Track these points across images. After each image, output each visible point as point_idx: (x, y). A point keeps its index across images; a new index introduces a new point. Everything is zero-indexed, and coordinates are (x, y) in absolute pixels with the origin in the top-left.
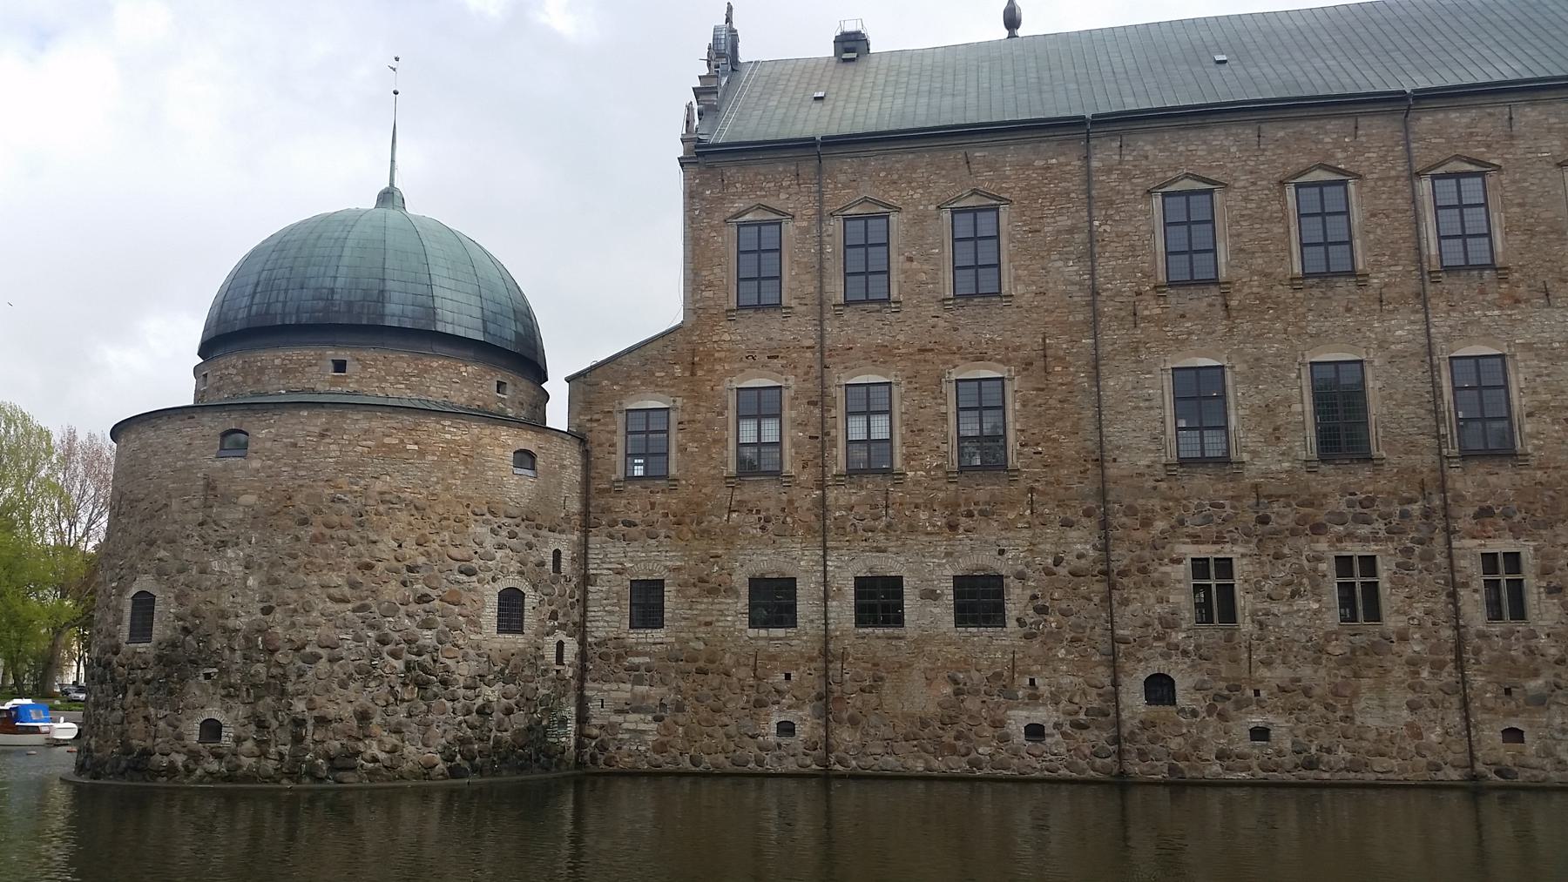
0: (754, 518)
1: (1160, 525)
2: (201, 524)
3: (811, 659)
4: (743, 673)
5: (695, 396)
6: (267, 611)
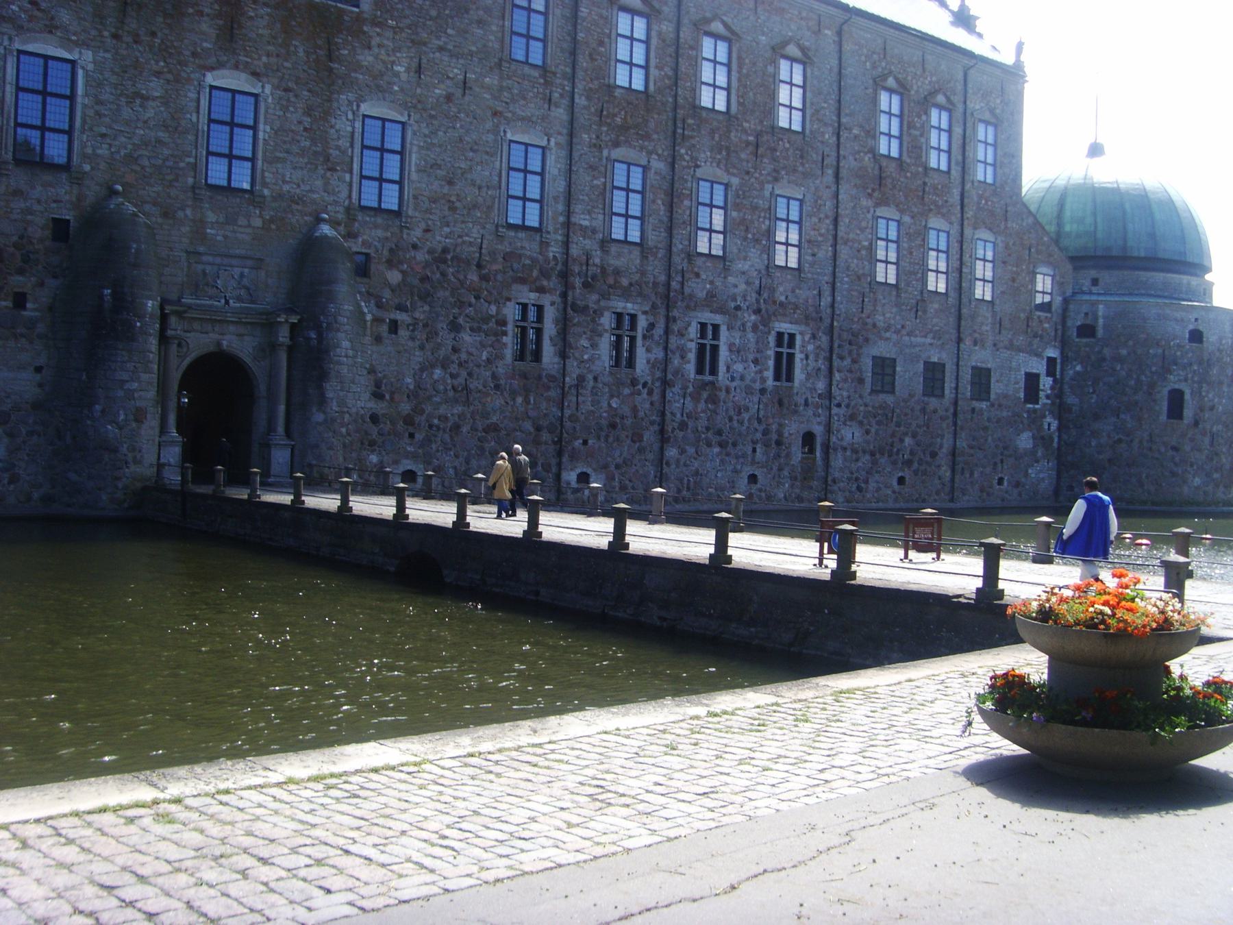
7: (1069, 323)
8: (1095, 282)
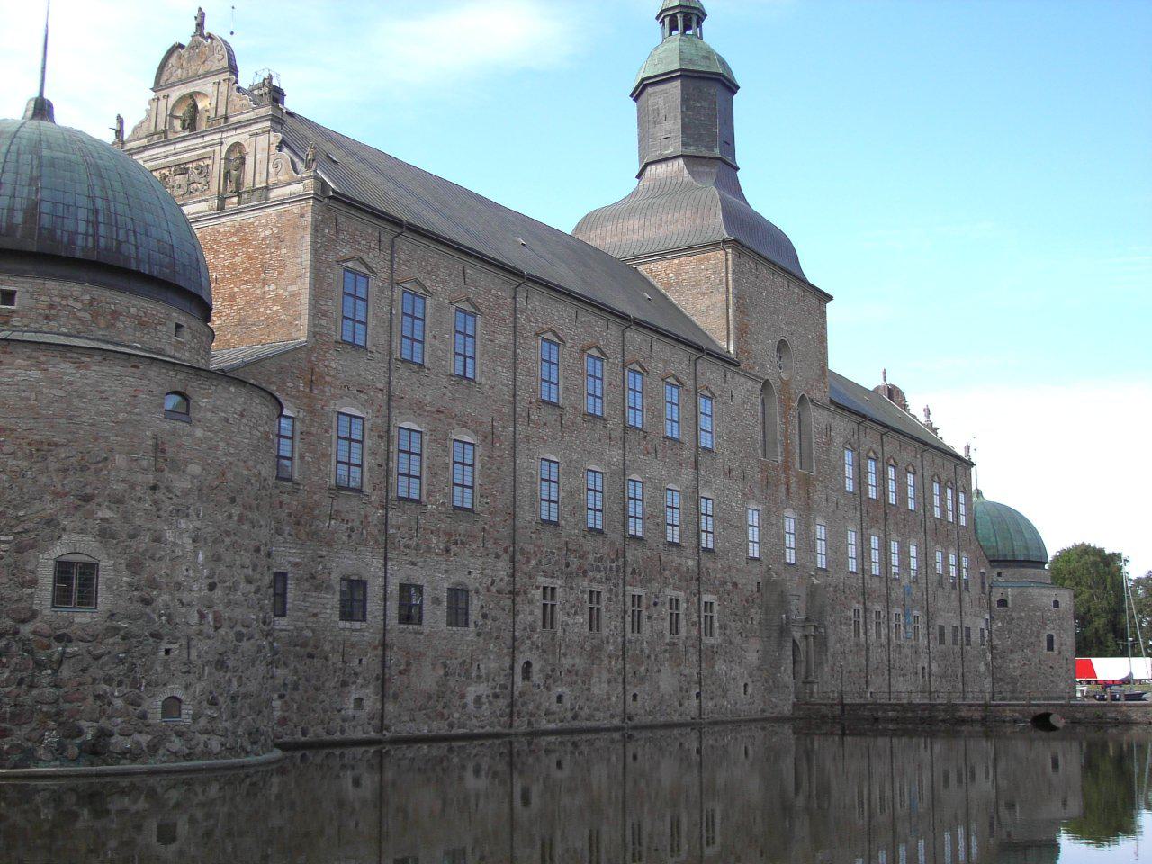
0: (344, 527)
1: (533, 562)
2: (154, 488)
3: (375, 648)
4: (335, 658)
5: (311, 411)
6: (212, 587)
7: (993, 599)
8: (999, 575)
